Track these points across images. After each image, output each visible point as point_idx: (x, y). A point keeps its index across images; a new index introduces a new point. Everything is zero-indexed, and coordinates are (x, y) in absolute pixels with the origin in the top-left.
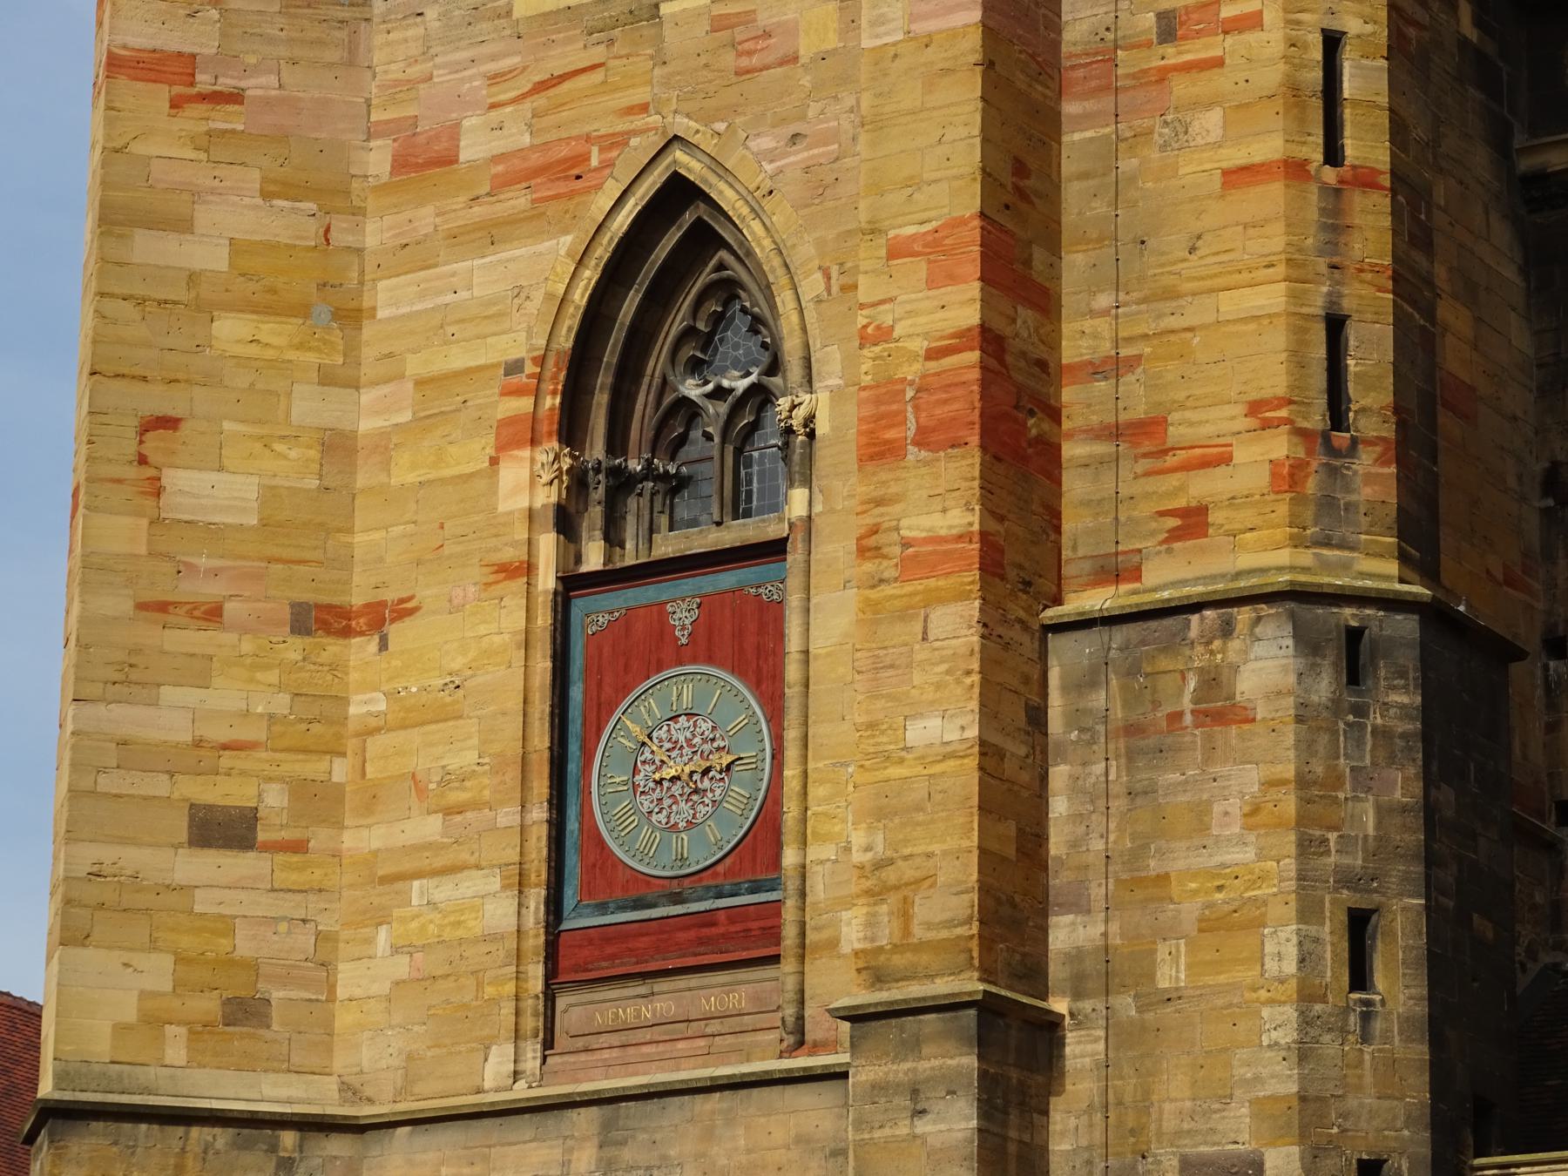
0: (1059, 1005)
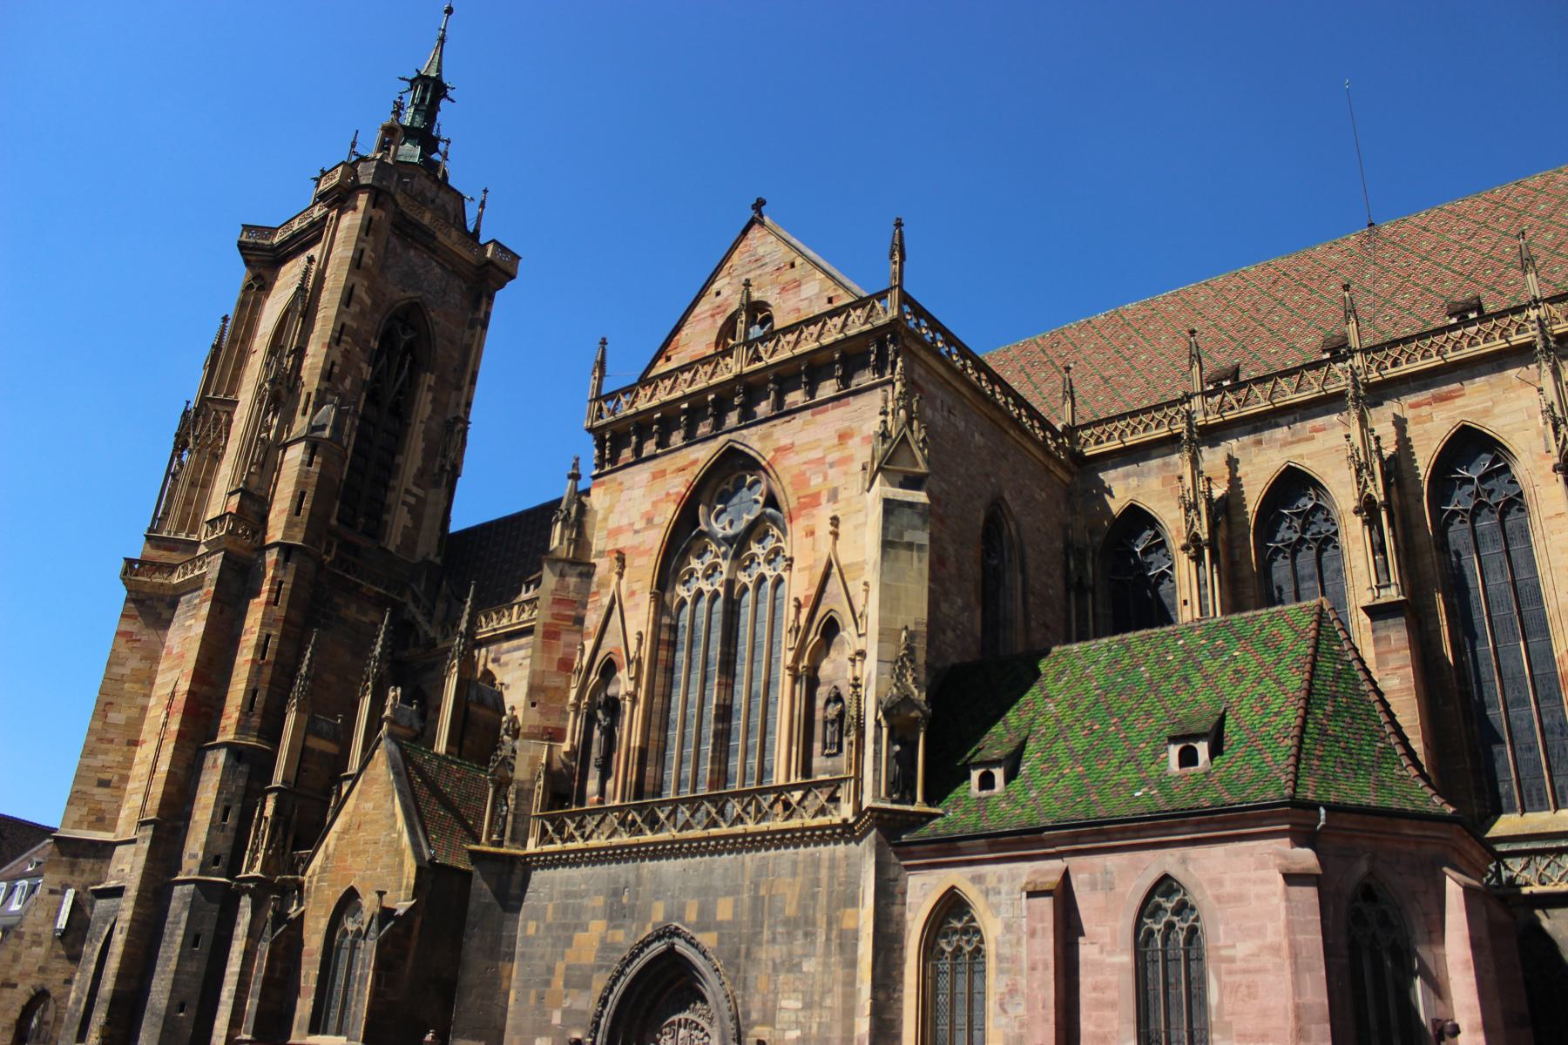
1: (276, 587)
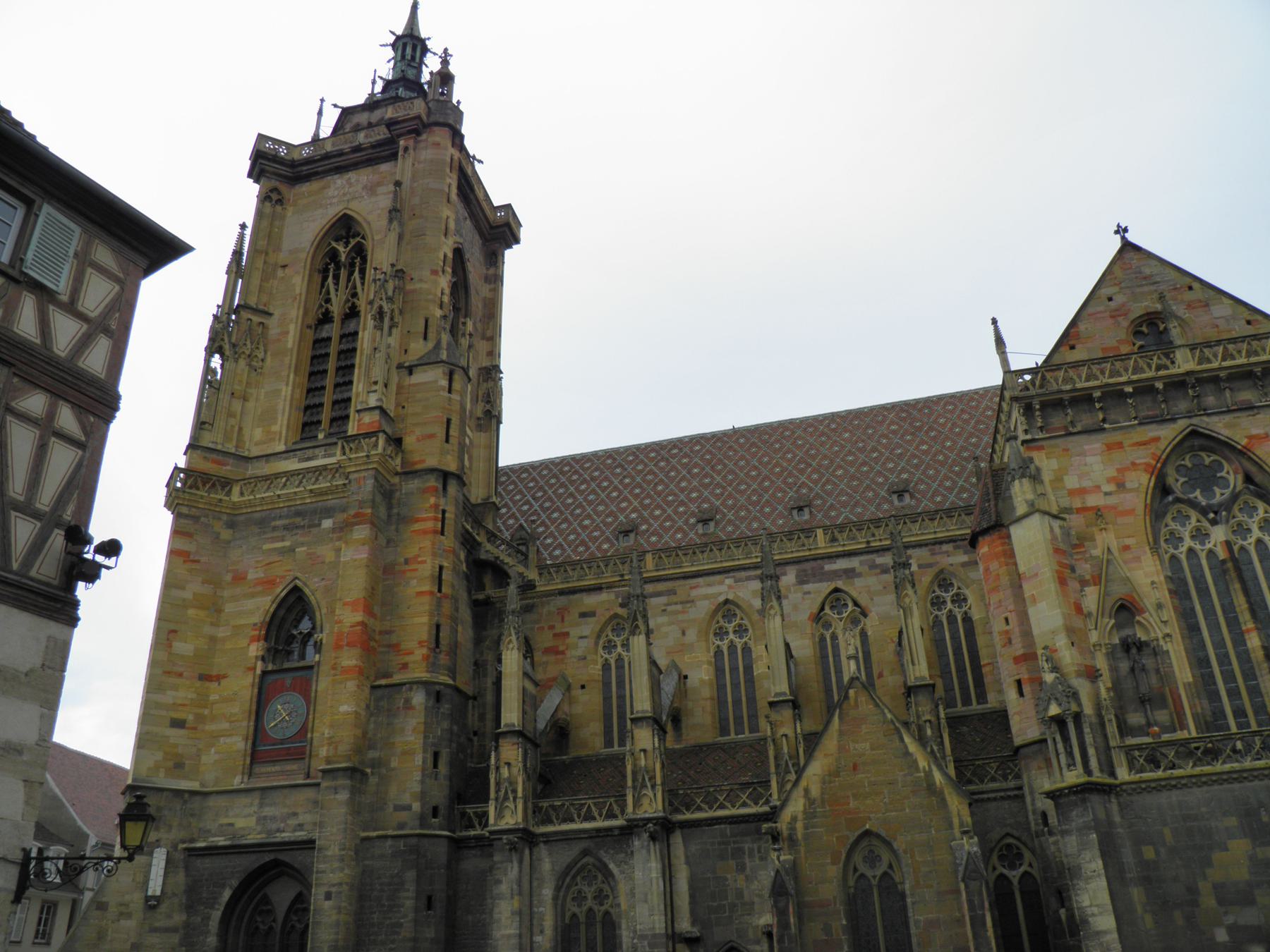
0: (369, 770)
1: (440, 516)
